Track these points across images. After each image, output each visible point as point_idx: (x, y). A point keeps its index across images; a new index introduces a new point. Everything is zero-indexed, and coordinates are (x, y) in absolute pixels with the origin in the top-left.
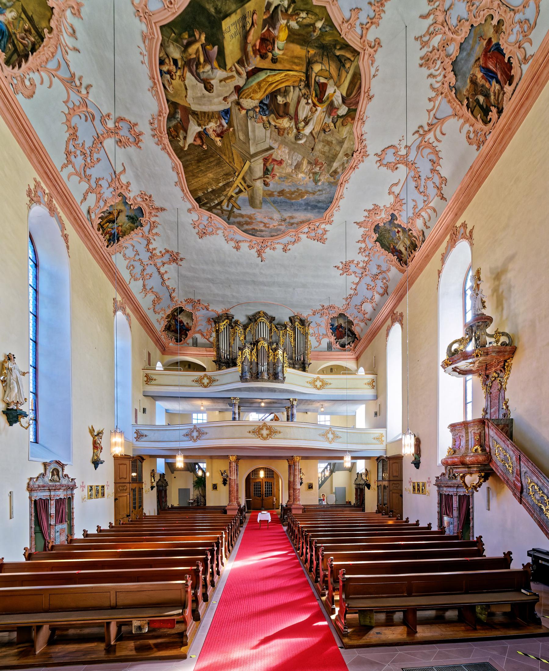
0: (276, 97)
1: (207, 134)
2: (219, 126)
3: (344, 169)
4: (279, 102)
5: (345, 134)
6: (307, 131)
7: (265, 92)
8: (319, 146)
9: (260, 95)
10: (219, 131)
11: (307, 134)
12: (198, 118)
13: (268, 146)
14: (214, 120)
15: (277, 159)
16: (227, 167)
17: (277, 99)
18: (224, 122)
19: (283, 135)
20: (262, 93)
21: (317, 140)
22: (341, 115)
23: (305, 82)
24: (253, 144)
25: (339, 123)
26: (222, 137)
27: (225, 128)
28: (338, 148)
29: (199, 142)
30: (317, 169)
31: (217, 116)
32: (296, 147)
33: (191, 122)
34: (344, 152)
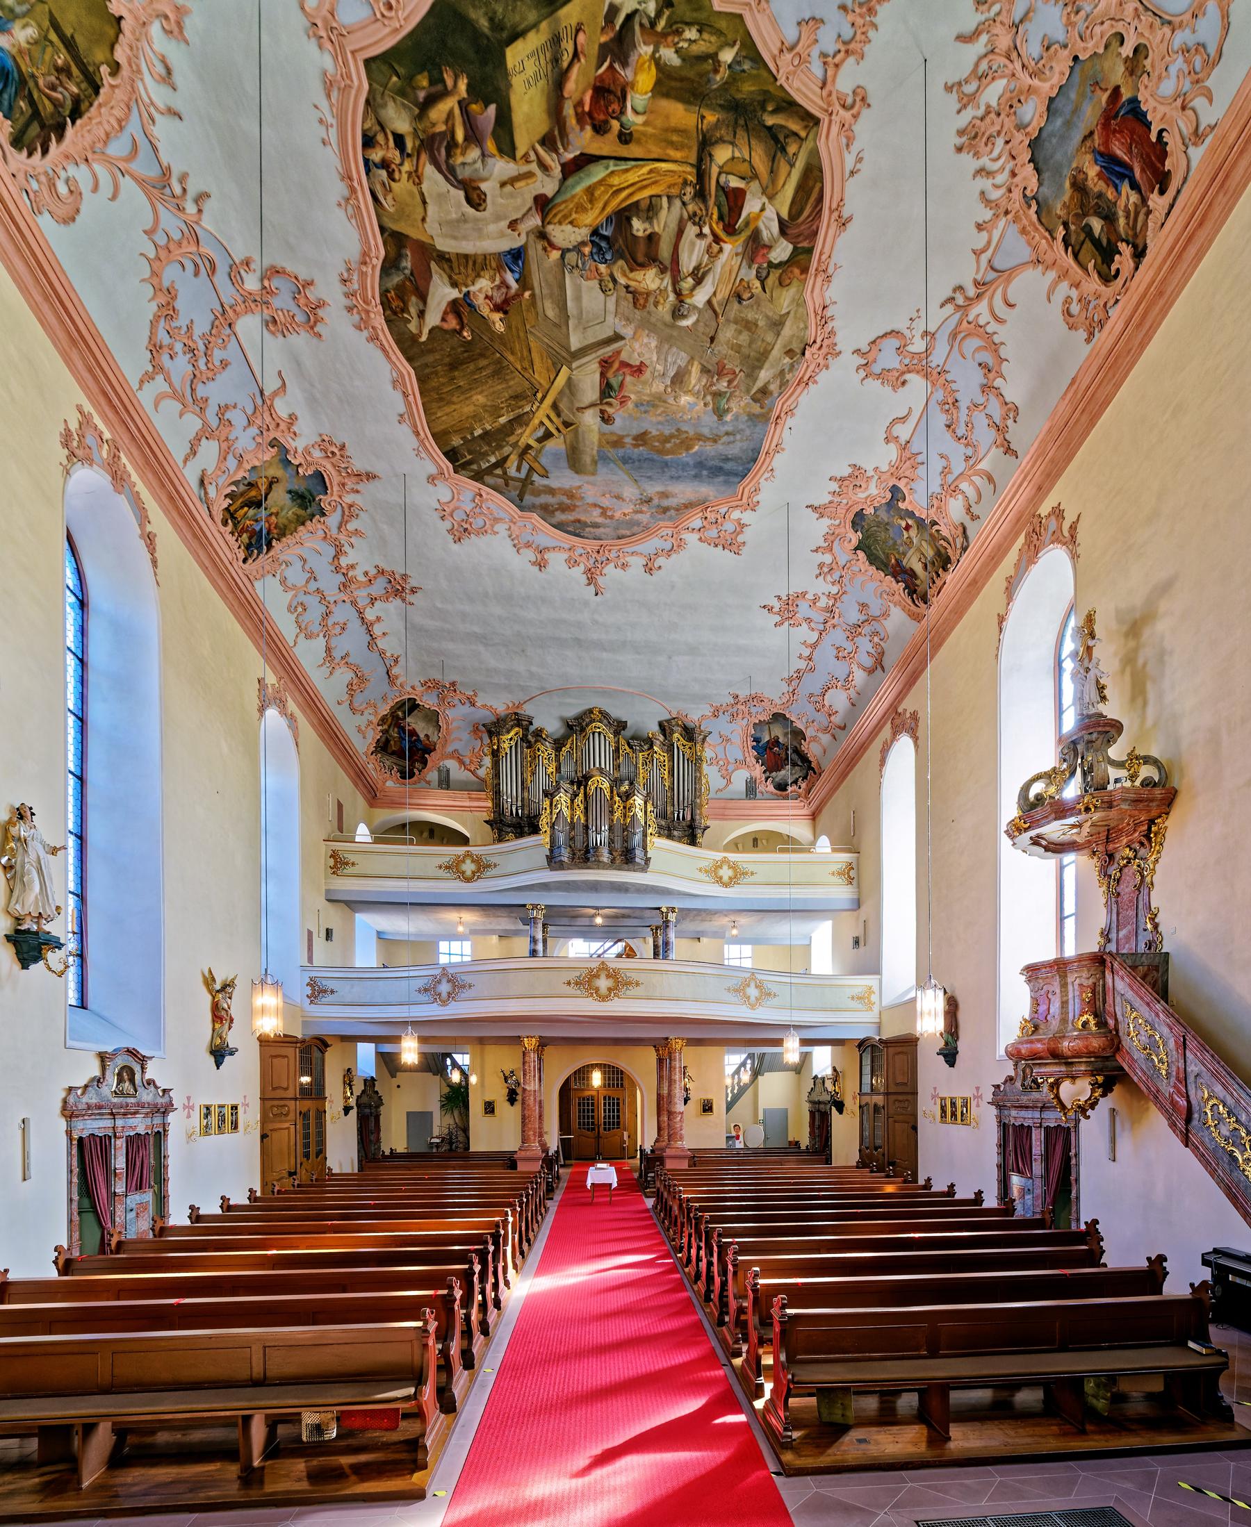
0: (629, 220)
1: (471, 305)
2: (499, 287)
3: (784, 385)
4: (635, 232)
5: (786, 304)
6: (700, 298)
7: (604, 208)
8: (727, 333)
9: (592, 217)
10: (498, 298)
11: (700, 305)
12: (451, 267)
13: (610, 333)
14: (487, 274)
15: (631, 362)
16: (517, 380)
17: (631, 226)
18: (510, 278)
19: (644, 307)
20: (597, 211)
21: (721, 320)
22: (776, 262)
23: (694, 187)
24: (576, 327)
25: (772, 280)
26: (506, 312)
27: (513, 291)
28: (769, 338)
29: (453, 323)
30: (723, 385)
31: (494, 265)
32: (675, 333)
33: (435, 277)
34: (785, 346)
